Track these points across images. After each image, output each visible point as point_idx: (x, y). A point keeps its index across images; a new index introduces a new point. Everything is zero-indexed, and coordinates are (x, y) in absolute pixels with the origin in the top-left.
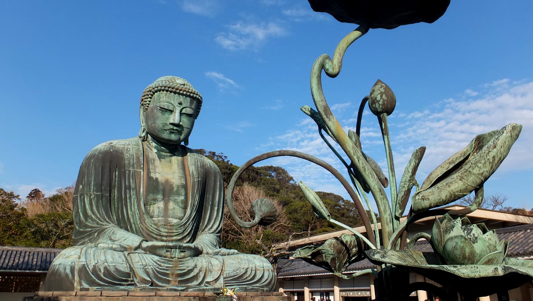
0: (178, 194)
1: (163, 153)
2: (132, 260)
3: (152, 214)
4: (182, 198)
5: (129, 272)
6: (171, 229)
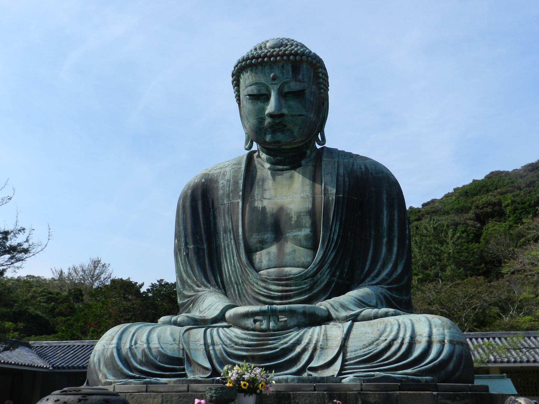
0: (299, 226)
2: (189, 337)
3: (259, 265)
4: (306, 231)
5: (181, 356)
6: (286, 285)
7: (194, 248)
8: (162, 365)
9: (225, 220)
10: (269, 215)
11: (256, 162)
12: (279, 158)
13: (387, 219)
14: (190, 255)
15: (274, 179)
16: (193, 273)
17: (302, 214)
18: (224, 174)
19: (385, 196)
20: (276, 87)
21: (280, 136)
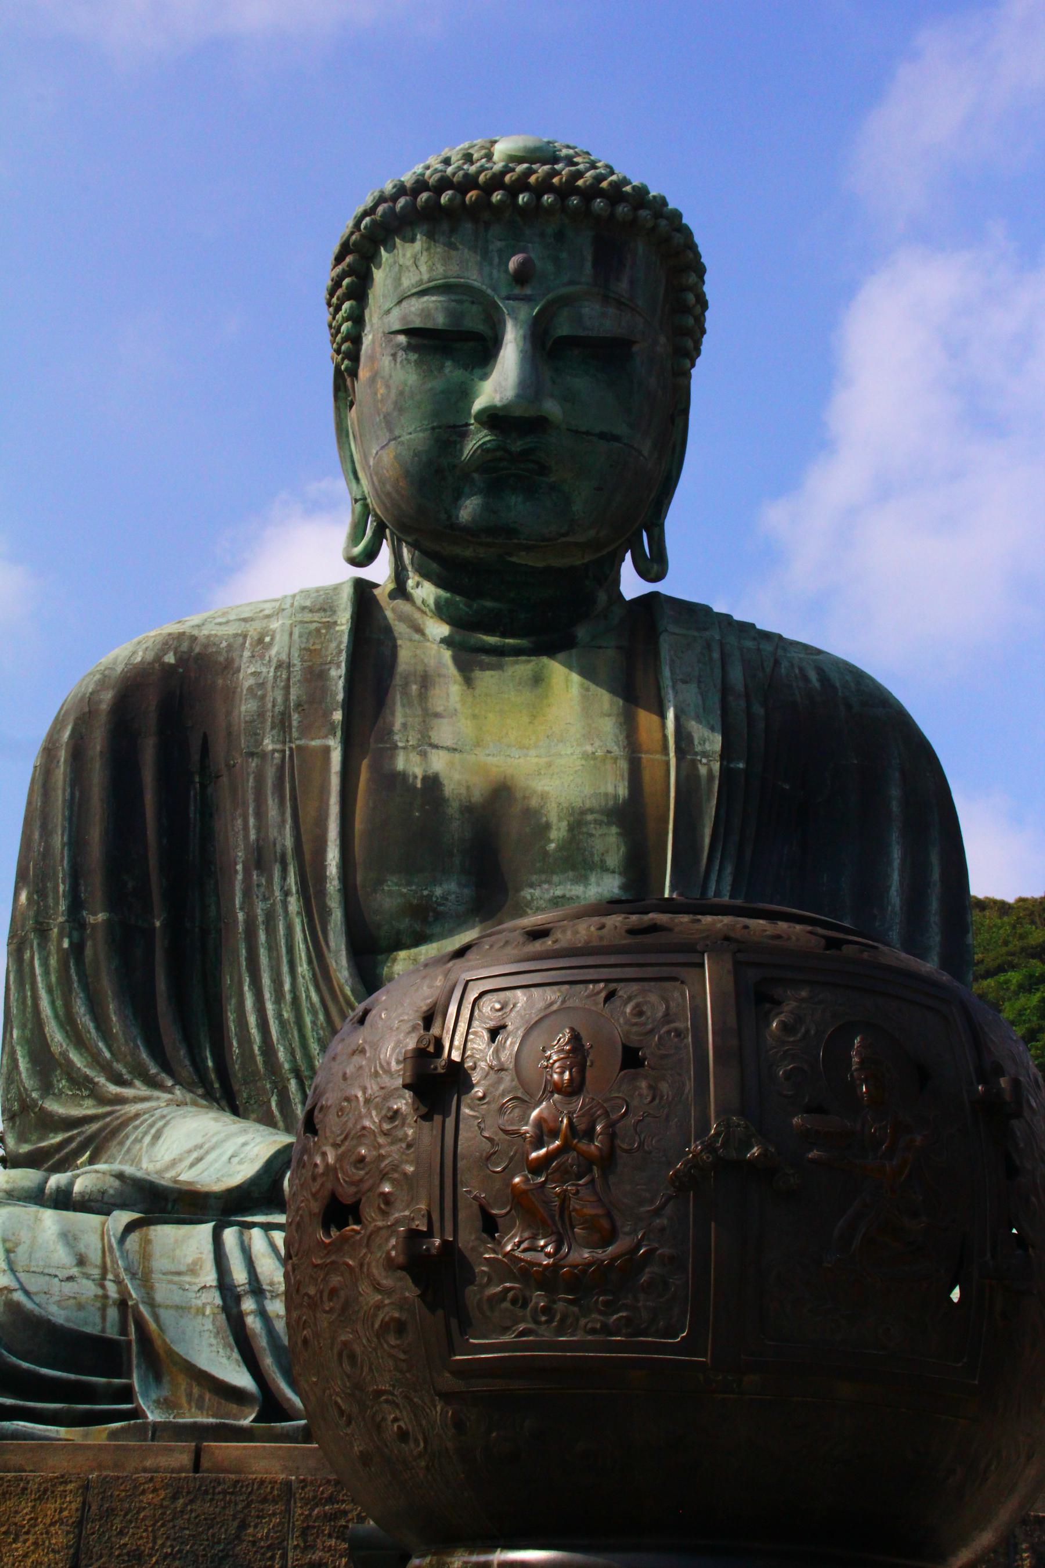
0: (576, 860)
1: (491, 640)
2: (146, 1254)
7: (108, 923)
8: (25, 1365)
9: (260, 815)
10: (453, 809)
11: (389, 614)
12: (489, 604)
13: (901, 876)
14: (88, 951)
15: (468, 682)
16: (98, 1028)
17: (590, 817)
18: (260, 641)
19: (895, 792)
20: (527, 312)
21: (517, 508)
